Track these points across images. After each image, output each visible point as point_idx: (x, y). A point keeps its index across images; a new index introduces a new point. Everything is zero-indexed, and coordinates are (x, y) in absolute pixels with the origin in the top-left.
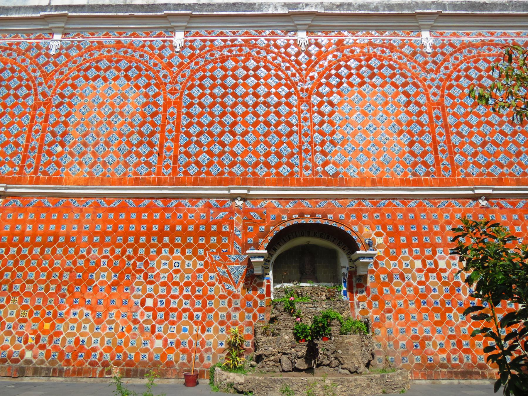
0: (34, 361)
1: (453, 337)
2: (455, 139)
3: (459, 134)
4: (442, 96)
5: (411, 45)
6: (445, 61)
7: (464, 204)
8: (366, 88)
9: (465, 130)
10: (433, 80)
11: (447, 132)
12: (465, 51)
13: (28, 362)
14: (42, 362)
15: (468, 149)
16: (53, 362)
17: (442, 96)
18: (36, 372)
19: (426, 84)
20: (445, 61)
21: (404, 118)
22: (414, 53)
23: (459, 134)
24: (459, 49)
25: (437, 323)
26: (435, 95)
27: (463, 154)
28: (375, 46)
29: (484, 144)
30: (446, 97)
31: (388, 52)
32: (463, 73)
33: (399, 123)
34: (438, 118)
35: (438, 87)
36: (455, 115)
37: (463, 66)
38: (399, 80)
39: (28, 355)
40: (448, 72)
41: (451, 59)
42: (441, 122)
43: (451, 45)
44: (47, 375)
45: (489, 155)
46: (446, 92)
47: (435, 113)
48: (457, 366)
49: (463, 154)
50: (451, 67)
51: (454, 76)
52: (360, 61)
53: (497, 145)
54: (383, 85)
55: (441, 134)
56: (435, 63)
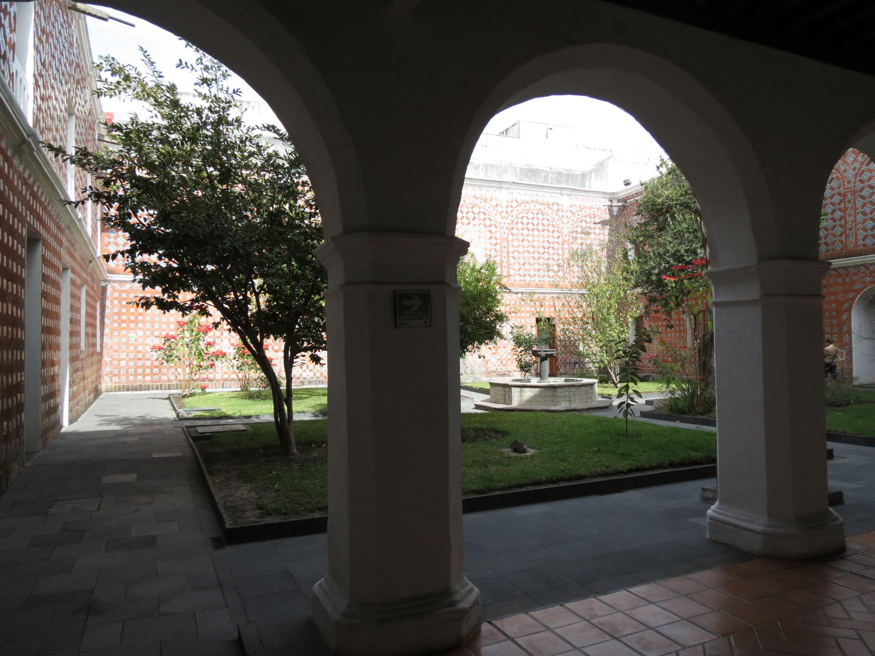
0: (308, 378)
1: (500, 359)
2: (511, 260)
3: (514, 258)
4: (508, 234)
5: (496, 200)
6: (512, 211)
7: (511, 296)
8: (471, 226)
9: (516, 255)
10: (505, 223)
11: (508, 256)
12: (523, 205)
13: (305, 378)
14: (312, 378)
15: (517, 267)
16: (318, 378)
17: (508, 234)
18: (310, 383)
19: (501, 226)
20: (512, 211)
21: (489, 246)
22: (497, 205)
23: (514, 258)
24: (520, 204)
25: (494, 354)
26: (505, 233)
27: (514, 269)
28: (477, 198)
29: (524, 264)
30: (510, 234)
31: (483, 202)
32: (520, 220)
33: (485, 249)
34: (504, 247)
35: (507, 228)
36: (513, 246)
37: (520, 216)
38: (488, 222)
39: (304, 375)
40: (513, 219)
41: (515, 210)
42: (505, 250)
43: (517, 201)
44: (315, 384)
45: (525, 270)
46: (510, 231)
47: (504, 244)
48: (500, 372)
49: (514, 269)
50: (514, 216)
51: (515, 222)
52: (468, 208)
53: (530, 264)
54: (479, 225)
55: (505, 257)
56: (507, 212)
